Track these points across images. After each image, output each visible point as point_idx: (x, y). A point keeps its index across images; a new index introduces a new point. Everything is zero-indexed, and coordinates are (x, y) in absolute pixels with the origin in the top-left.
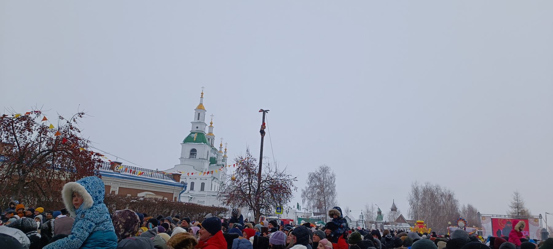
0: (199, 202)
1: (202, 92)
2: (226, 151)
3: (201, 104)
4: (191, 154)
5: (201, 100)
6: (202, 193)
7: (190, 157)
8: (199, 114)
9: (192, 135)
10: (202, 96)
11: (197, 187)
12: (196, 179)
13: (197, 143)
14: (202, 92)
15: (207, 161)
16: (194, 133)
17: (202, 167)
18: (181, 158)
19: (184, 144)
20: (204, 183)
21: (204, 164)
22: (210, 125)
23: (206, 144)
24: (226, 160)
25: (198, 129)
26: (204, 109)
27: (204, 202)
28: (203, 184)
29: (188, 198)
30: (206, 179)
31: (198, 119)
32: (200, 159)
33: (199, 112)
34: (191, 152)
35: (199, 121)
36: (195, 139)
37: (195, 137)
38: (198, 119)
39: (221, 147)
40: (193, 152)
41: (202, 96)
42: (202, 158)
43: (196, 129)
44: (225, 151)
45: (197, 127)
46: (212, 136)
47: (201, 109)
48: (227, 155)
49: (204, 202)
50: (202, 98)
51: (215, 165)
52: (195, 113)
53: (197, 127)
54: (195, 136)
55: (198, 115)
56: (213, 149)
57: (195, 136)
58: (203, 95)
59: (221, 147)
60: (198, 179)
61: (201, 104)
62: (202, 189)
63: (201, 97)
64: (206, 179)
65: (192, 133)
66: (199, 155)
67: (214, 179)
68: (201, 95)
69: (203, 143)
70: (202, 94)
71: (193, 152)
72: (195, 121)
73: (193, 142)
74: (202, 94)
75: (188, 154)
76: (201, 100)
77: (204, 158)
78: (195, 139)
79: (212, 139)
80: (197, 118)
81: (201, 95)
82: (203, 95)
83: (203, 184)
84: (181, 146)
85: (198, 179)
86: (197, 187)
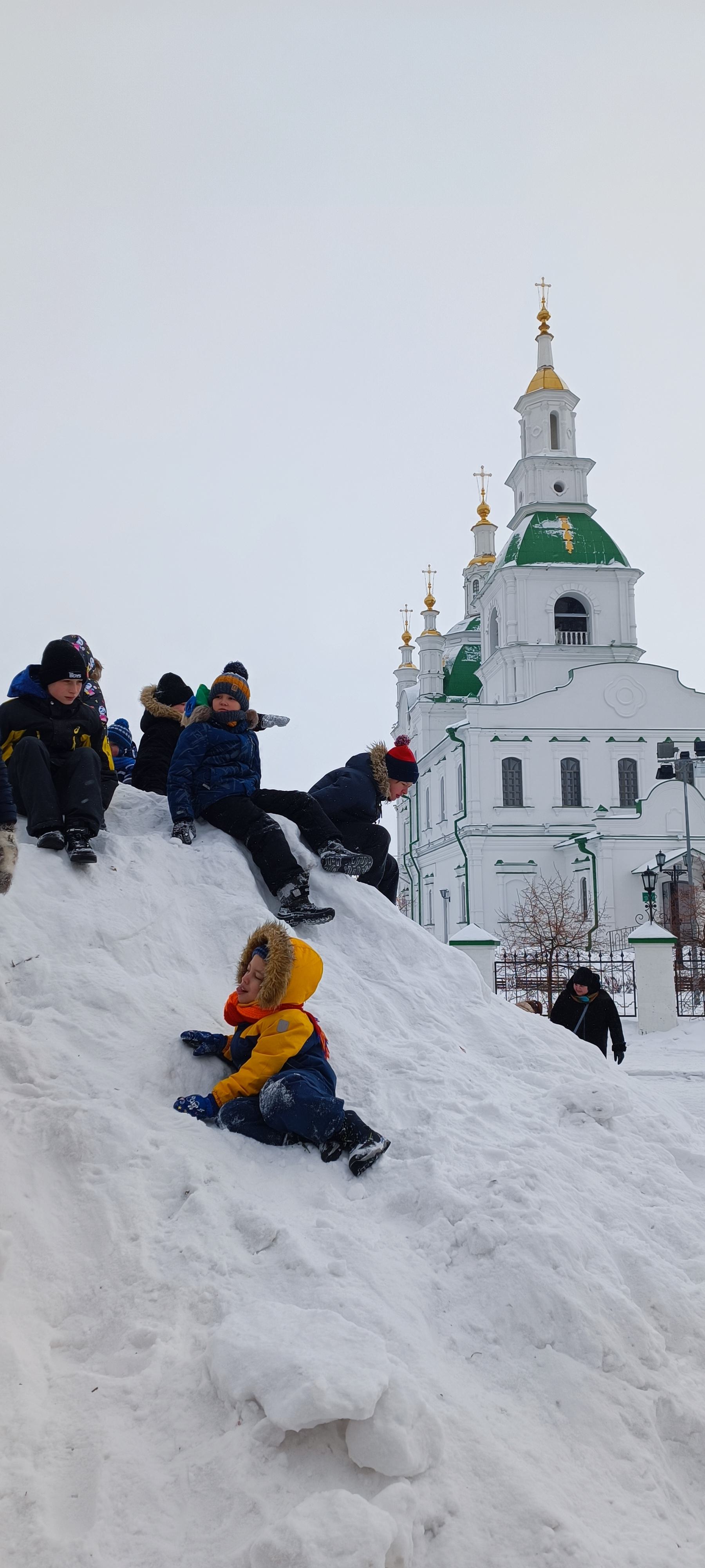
1: (544, 308)
3: (546, 368)
4: (561, 624)
5: (544, 352)
9: (547, 524)
14: (544, 308)
16: (552, 516)
19: (520, 570)
22: (480, 519)
25: (565, 497)
31: (555, 445)
33: (552, 409)
35: (555, 454)
38: (555, 445)
54: (562, 528)
55: (548, 420)
61: (546, 368)
70: (544, 316)
73: (567, 561)
74: (544, 316)
76: (544, 352)
78: (569, 546)
82: (547, 323)
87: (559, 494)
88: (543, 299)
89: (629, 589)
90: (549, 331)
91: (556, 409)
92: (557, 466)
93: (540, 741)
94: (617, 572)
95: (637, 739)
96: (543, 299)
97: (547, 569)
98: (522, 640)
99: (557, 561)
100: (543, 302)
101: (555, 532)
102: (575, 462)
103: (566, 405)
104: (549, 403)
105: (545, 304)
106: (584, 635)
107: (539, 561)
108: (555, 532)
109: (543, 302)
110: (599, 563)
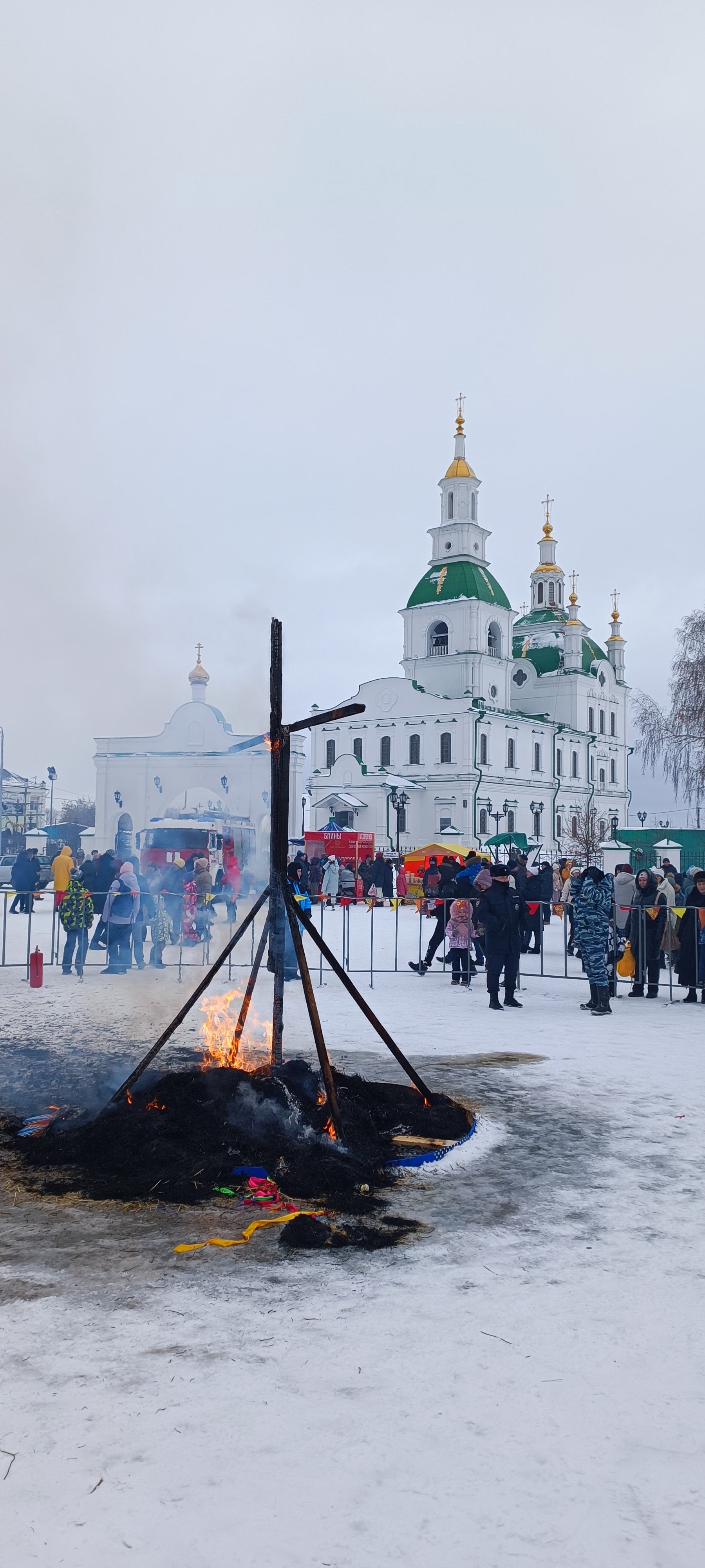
0: (438, 801)
1: (460, 416)
2: (618, 620)
5: (460, 446)
6: (445, 769)
7: (430, 654)
8: (451, 496)
9: (434, 575)
10: (460, 428)
11: (430, 750)
12: (423, 722)
13: (444, 602)
14: (460, 416)
15: (485, 658)
17: (467, 682)
18: (407, 659)
20: (418, 736)
21: (476, 669)
22: (545, 535)
23: (474, 598)
24: (616, 652)
25: (453, 551)
26: (469, 475)
27: (453, 801)
28: (446, 739)
29: (380, 789)
30: (454, 720)
31: (451, 516)
32: (459, 654)
33: (449, 491)
35: (452, 522)
36: (439, 589)
37: (441, 581)
38: (451, 516)
39: (573, 605)
41: (460, 428)
42: (466, 649)
43: (444, 553)
44: (612, 620)
45: (449, 546)
46: (550, 574)
47: (456, 476)
48: (623, 632)
49: (453, 801)
51: (554, 673)
52: (442, 495)
53: (449, 546)
55: (446, 500)
56: (553, 618)
57: (440, 576)
58: (462, 425)
59: (573, 605)
60: (430, 723)
61: (459, 459)
62: (446, 756)
63: (456, 432)
64: (454, 720)
65: (436, 568)
67: (482, 717)
68: (457, 426)
69: (463, 598)
70: (460, 421)
72: (443, 525)
73: (434, 601)
74: (460, 421)
75: (422, 644)
76: (460, 446)
77: (474, 648)
78: (439, 589)
79: (551, 584)
80: (446, 514)
81: (457, 426)
82: (462, 425)
83: (446, 739)
84: (401, 619)
85: (430, 723)
86: (430, 750)
87: (448, 550)
88: (460, 408)
89: (471, 613)
90: (464, 432)
92: (446, 532)
94: (461, 603)
95: (391, 724)
96: (460, 408)
97: (421, 608)
98: (409, 656)
99: (428, 602)
100: (460, 411)
101: (435, 580)
102: (456, 527)
103: (460, 485)
104: (448, 487)
105: (462, 412)
106: (447, 647)
107: (419, 603)
108: (435, 580)
109: (460, 411)
110: (453, 598)
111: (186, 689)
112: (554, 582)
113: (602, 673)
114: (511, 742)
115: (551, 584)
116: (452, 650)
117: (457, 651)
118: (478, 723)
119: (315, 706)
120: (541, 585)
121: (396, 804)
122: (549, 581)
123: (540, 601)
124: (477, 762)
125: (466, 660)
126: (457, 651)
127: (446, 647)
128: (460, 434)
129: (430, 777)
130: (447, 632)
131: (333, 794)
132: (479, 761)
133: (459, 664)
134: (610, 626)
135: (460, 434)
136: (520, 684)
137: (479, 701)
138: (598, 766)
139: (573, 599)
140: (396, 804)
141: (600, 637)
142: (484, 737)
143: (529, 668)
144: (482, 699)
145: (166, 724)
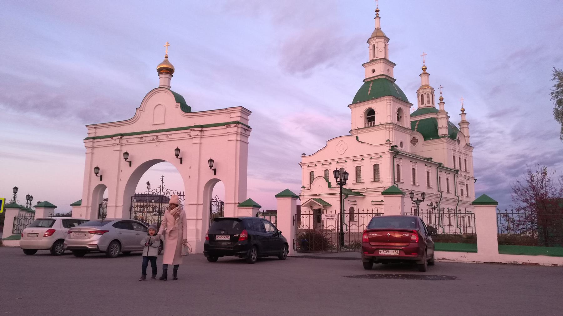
0: (373, 203)
1: (377, 9)
14: (377, 9)
25: (376, 74)
28: (376, 168)
34: (368, 116)
40: (370, 115)
45: (374, 71)
50: (377, 19)
53: (374, 71)
60: (367, 159)
63: (376, 16)
66: (379, 119)
68: (376, 13)
70: (377, 11)
71: (370, 115)
74: (377, 11)
75: (361, 122)
82: (379, 13)
83: (376, 168)
85: (367, 159)
90: (379, 16)
91: (374, 43)
93: (319, 165)
106: (375, 122)
111: (157, 80)
112: (429, 94)
113: (458, 138)
114: (414, 169)
115: (428, 94)
116: (377, 122)
117: (380, 123)
118: (395, 158)
119: (304, 154)
120: (422, 96)
121: (338, 180)
122: (427, 94)
123: (423, 103)
124: (395, 180)
125: (385, 127)
126: (380, 123)
127: (374, 122)
128: (378, 17)
129: (368, 189)
130: (374, 114)
131: (311, 199)
132: (396, 180)
133: (382, 130)
134: (460, 115)
135: (378, 17)
136: (414, 144)
137: (394, 147)
138: (459, 187)
139: (441, 99)
140: (338, 180)
141: (455, 119)
142: (398, 166)
143: (419, 137)
144: (396, 146)
145: (137, 108)
